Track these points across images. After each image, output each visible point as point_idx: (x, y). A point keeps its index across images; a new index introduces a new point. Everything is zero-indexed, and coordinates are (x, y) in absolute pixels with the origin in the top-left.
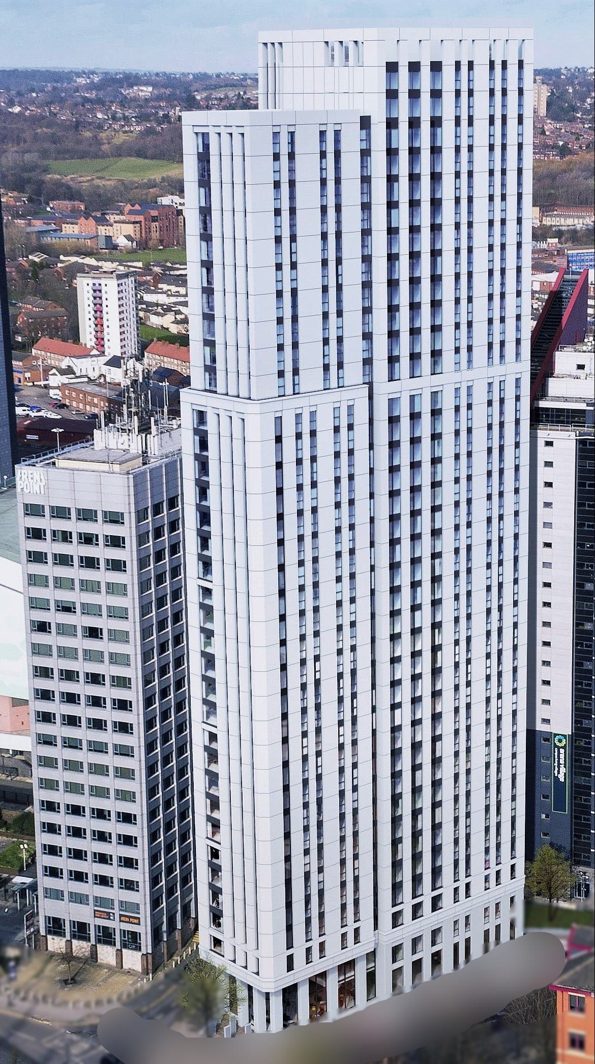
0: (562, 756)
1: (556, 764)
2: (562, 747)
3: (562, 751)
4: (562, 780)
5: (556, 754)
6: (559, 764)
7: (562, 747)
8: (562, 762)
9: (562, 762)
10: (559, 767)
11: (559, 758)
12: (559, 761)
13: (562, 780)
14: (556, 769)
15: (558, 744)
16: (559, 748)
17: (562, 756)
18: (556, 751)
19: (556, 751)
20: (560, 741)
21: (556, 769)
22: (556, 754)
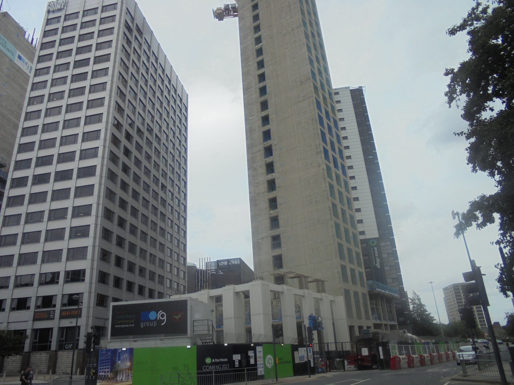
0: (376, 252)
1: (373, 258)
2: (375, 246)
3: (375, 248)
4: (379, 267)
5: (372, 251)
6: (375, 257)
7: (375, 246)
8: (377, 255)
9: (377, 255)
10: (375, 259)
11: (374, 253)
12: (375, 255)
13: (379, 267)
14: (374, 261)
15: (372, 245)
16: (373, 247)
17: (376, 252)
18: (372, 249)
19: (372, 249)
20: (373, 242)
21: (374, 261)
22: (372, 251)
